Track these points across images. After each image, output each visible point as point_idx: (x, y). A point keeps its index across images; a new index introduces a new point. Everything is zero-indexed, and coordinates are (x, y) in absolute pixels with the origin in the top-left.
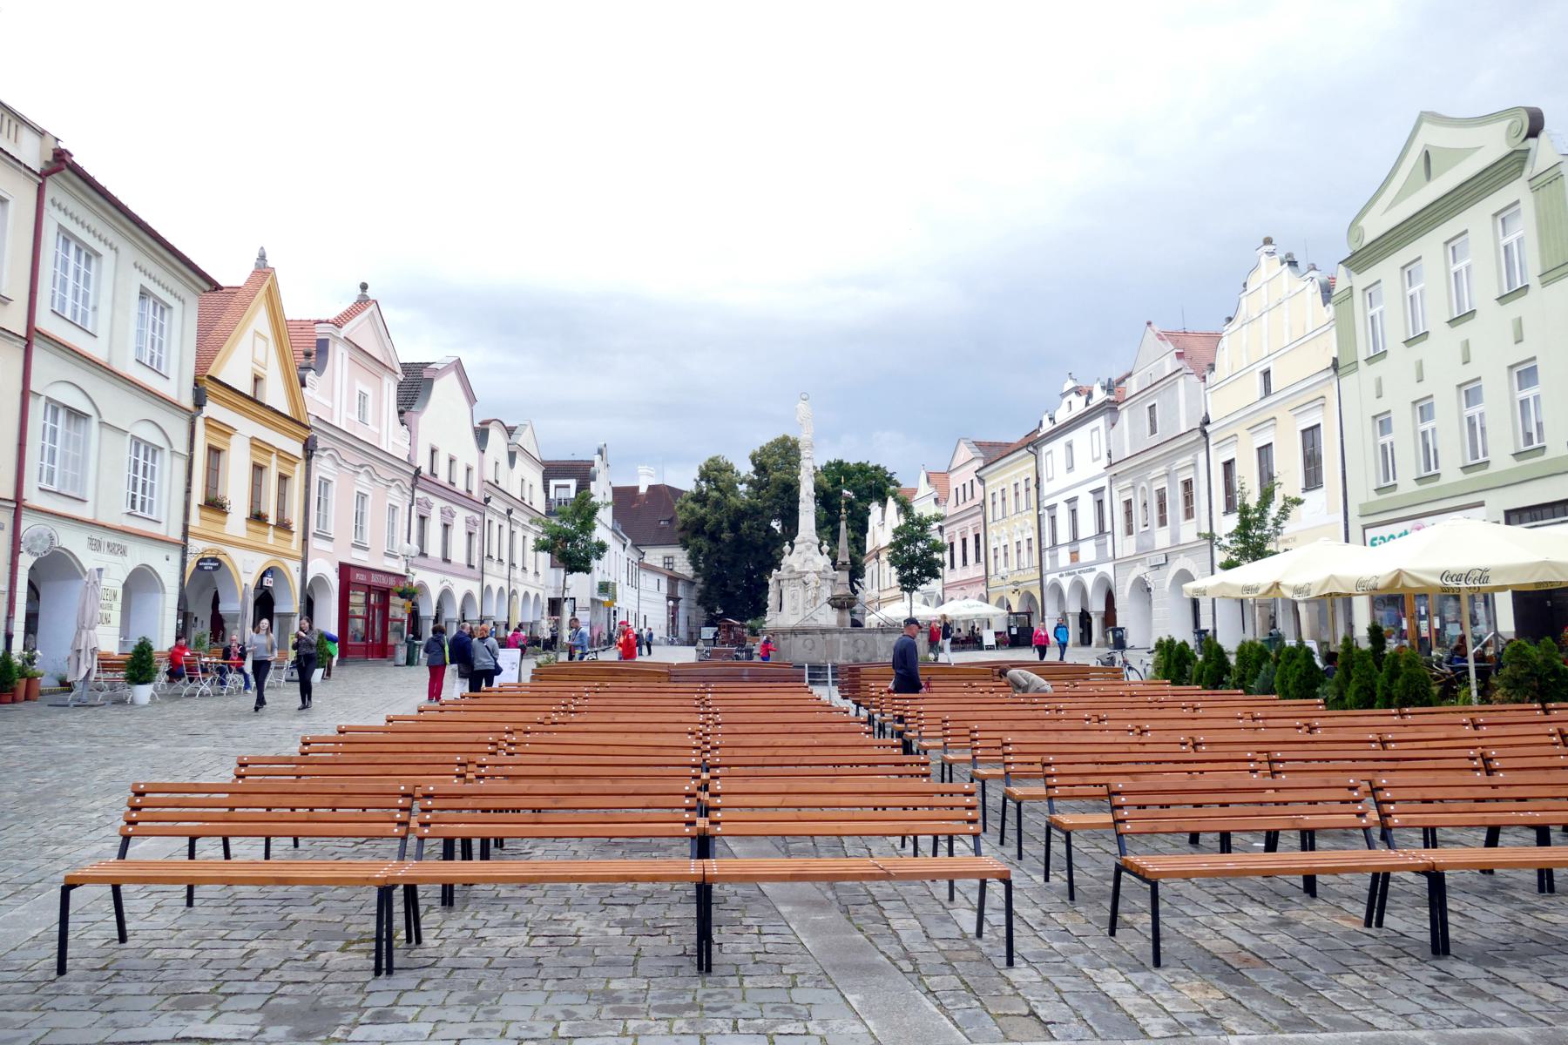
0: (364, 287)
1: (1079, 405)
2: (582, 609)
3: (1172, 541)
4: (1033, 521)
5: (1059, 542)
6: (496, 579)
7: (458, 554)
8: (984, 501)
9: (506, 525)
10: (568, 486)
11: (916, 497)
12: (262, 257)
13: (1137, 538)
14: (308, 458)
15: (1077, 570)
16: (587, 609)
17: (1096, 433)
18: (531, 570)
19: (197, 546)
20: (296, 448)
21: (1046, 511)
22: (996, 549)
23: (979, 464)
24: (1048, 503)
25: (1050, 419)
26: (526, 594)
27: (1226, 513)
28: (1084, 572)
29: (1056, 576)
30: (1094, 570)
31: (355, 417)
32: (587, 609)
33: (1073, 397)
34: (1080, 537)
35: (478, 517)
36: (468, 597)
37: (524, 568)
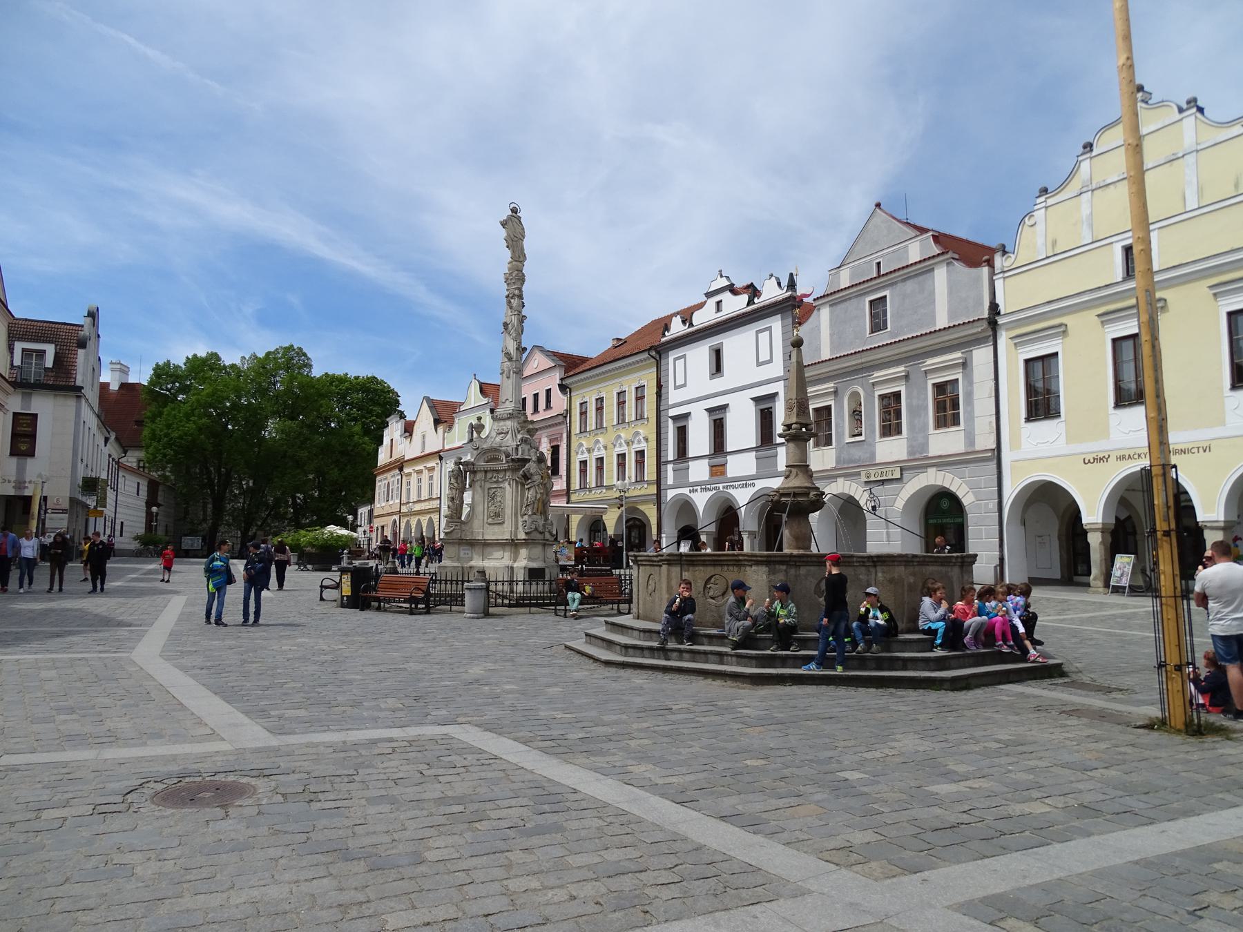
1: (735, 305)
2: (55, 511)
3: (909, 453)
4: (649, 430)
5: (691, 453)
8: (569, 411)
10: (44, 352)
11: (462, 408)
13: (839, 451)
15: (721, 486)
16: (64, 511)
17: (764, 336)
21: (670, 421)
22: (584, 463)
24: (673, 412)
25: (684, 322)
27: (1028, 420)
28: (734, 487)
29: (686, 491)
30: (753, 485)
32: (64, 511)
33: (726, 297)
34: (730, 447)
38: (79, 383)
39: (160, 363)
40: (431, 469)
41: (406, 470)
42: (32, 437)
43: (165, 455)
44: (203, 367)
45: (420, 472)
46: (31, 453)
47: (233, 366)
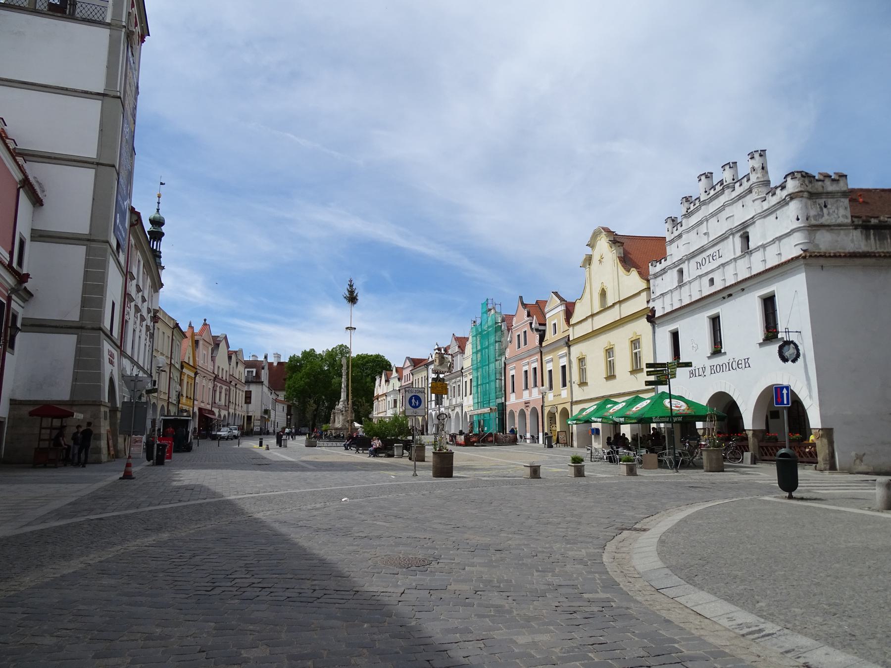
0: (205, 320)
2: (257, 420)
5: (432, 400)
6: (231, 411)
7: (223, 402)
8: (413, 382)
9: (235, 389)
10: (253, 371)
12: (190, 323)
14: (195, 378)
16: (259, 420)
18: (240, 405)
19: (180, 405)
20: (192, 375)
23: (411, 368)
26: (239, 415)
29: (431, 411)
31: (203, 362)
32: (259, 420)
35: (228, 388)
36: (225, 416)
37: (238, 405)
38: (262, 380)
39: (292, 356)
40: (384, 400)
41: (379, 400)
42: (250, 397)
43: (293, 395)
44: (309, 355)
45: (382, 400)
46: (250, 403)
47: (320, 354)
